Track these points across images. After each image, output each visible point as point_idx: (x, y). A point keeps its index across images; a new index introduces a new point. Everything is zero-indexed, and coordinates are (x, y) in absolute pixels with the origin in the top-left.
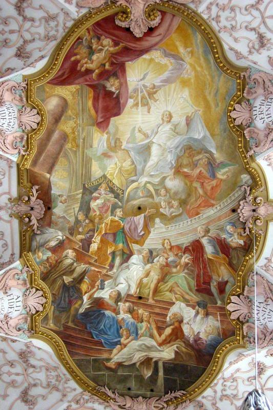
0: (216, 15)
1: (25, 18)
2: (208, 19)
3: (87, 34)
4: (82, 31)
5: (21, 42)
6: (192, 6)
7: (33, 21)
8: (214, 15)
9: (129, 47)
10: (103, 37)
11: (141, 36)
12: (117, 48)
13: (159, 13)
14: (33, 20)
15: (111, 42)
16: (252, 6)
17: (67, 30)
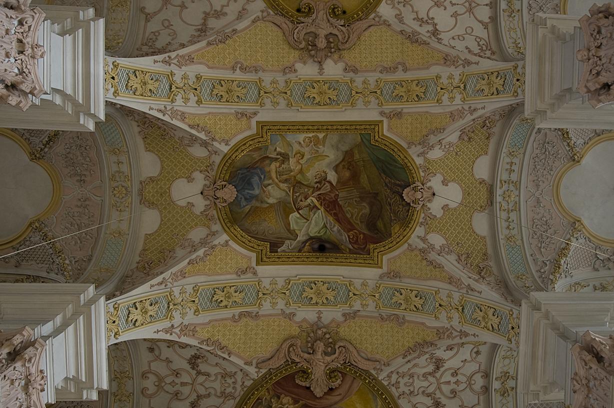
0: (395, 380)
1: (199, 373)
2: (388, 385)
3: (267, 394)
4: (263, 392)
5: (194, 397)
6: (374, 372)
7: (208, 375)
8: (393, 380)
9: (308, 404)
10: (283, 396)
11: (321, 395)
12: (297, 405)
13: (340, 375)
14: (208, 375)
15: (290, 399)
16: (430, 374)
17: (245, 389)
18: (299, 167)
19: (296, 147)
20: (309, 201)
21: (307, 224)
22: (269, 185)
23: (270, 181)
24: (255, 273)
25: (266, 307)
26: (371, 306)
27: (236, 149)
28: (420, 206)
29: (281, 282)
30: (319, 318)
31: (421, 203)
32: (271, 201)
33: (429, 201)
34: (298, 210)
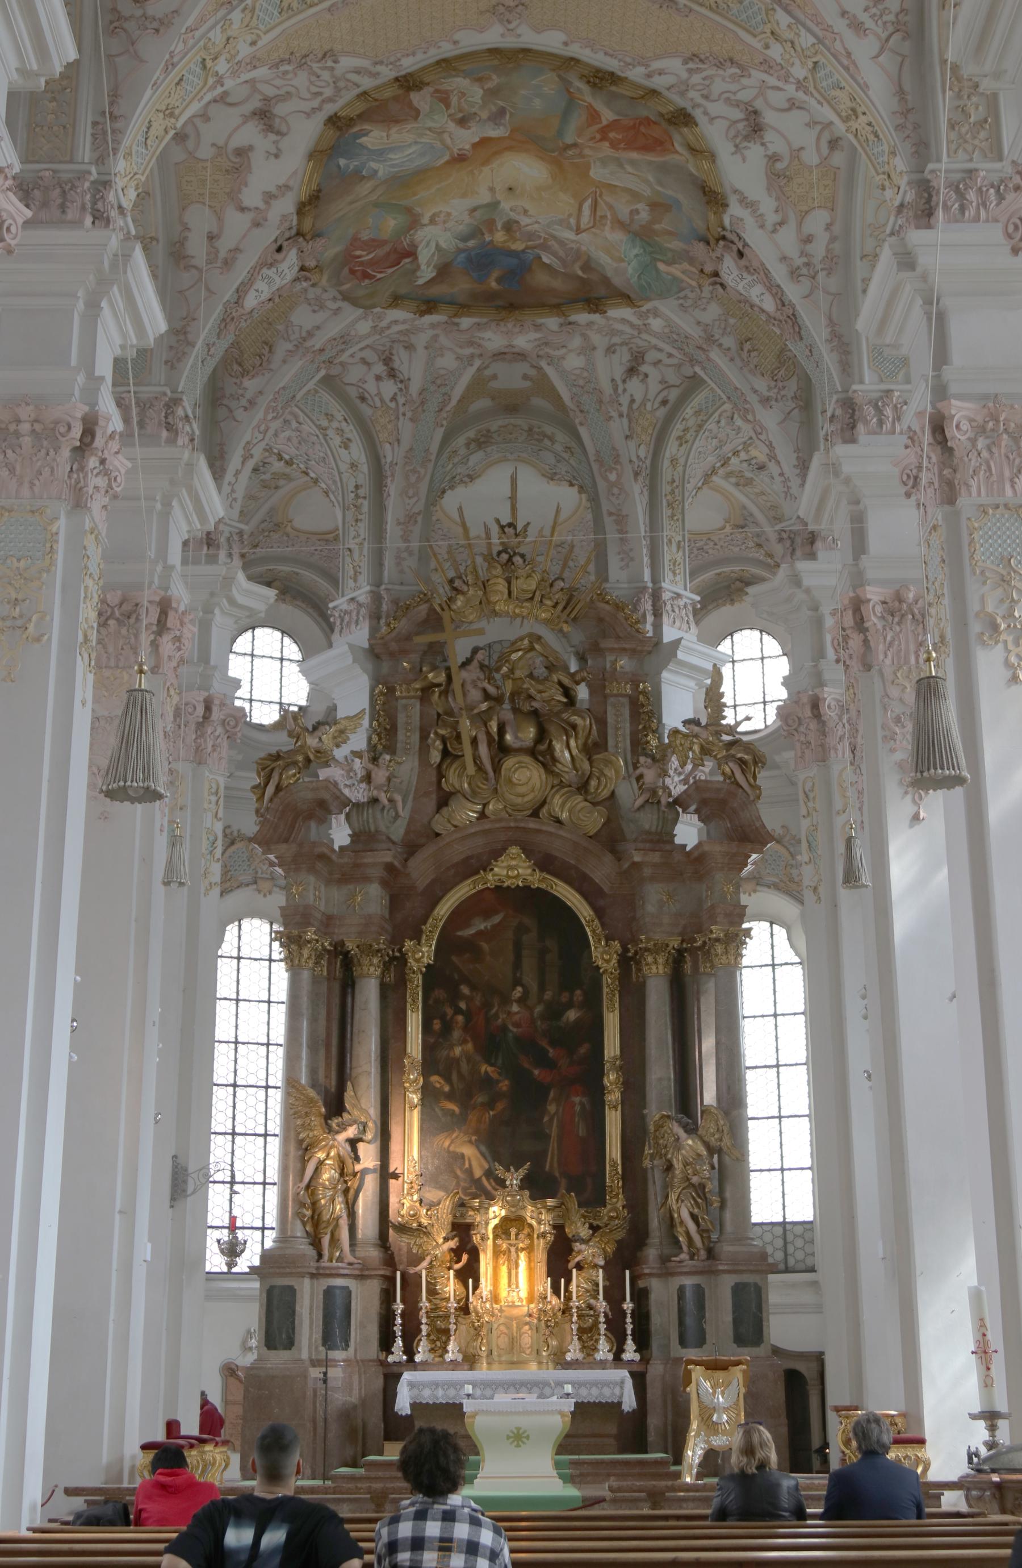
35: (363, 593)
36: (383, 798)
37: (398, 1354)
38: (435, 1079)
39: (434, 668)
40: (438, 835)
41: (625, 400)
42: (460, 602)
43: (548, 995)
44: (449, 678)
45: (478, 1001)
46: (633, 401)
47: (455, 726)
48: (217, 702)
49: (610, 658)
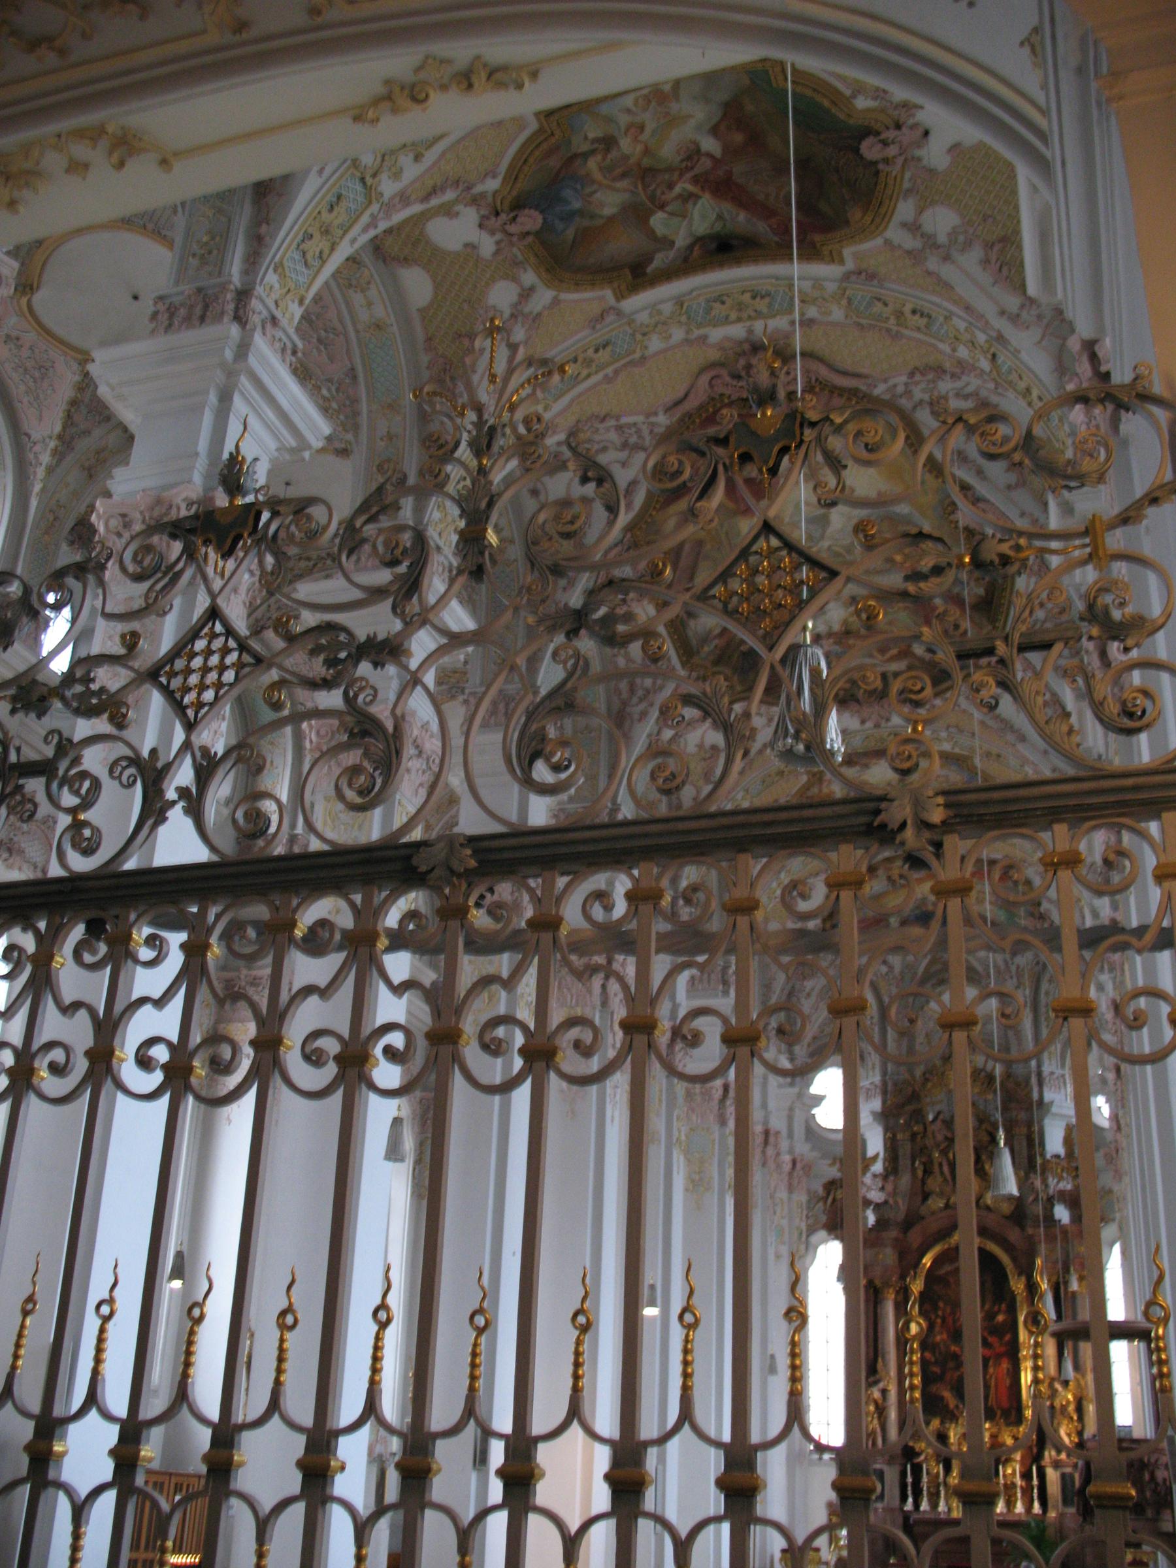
6: (863, 388)
18: (639, 148)
19: (624, 119)
20: (677, 189)
21: (685, 223)
22: (595, 192)
23: (595, 187)
24: (619, 313)
25: (655, 344)
26: (838, 314)
27: (513, 175)
28: (898, 167)
29: (667, 308)
30: (750, 331)
31: (900, 160)
32: (608, 211)
33: (919, 147)
34: (662, 207)
35: (877, 1079)
36: (891, 1201)
37: (909, 1505)
38: (927, 1355)
39: (917, 1122)
40: (923, 1218)
41: (1013, 969)
42: (929, 1085)
43: (987, 1307)
44: (925, 1129)
45: (948, 1310)
46: (1018, 967)
47: (930, 1156)
48: (798, 1160)
49: (1014, 1114)
